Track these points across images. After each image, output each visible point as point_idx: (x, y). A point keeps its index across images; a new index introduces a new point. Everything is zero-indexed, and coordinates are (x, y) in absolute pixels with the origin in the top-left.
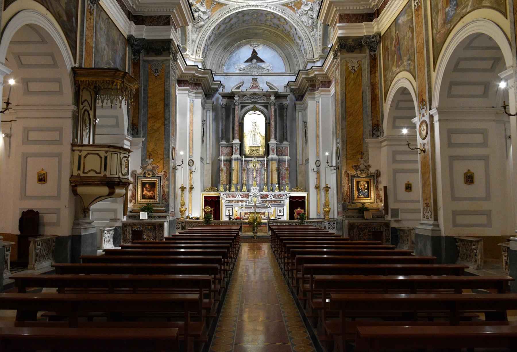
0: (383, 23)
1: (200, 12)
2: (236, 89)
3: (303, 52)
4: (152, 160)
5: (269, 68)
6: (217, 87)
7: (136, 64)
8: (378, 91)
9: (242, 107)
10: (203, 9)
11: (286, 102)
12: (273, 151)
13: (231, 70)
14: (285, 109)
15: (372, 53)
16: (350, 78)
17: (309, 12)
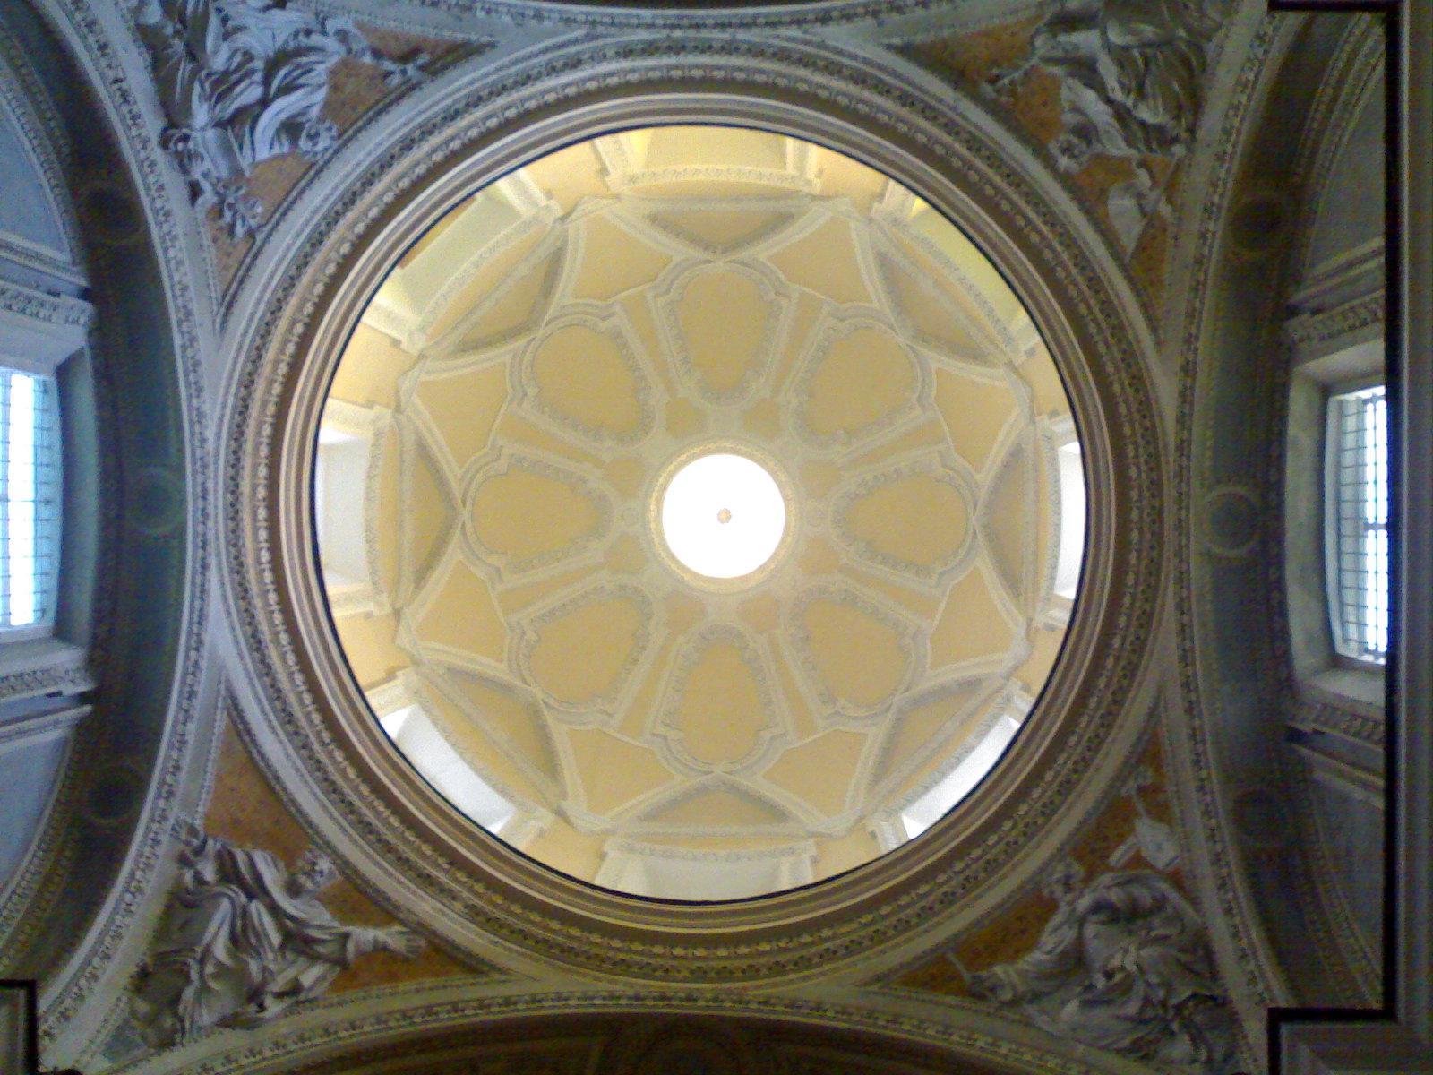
17: (249, 93)
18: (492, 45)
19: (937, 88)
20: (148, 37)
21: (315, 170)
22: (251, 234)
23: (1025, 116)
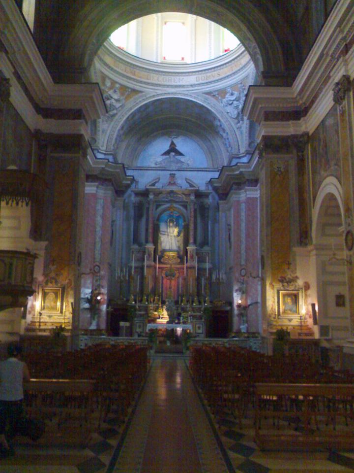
1: (113, 101)
2: (150, 186)
3: (228, 145)
4: (55, 267)
5: (189, 162)
6: (129, 182)
7: (41, 159)
8: (306, 195)
9: (158, 206)
10: (115, 96)
11: (209, 201)
13: (146, 164)
16: (277, 180)
17: (235, 102)
19: (138, 88)
20: (242, 120)
21: (231, 86)
22: (241, 83)
23: (123, 88)
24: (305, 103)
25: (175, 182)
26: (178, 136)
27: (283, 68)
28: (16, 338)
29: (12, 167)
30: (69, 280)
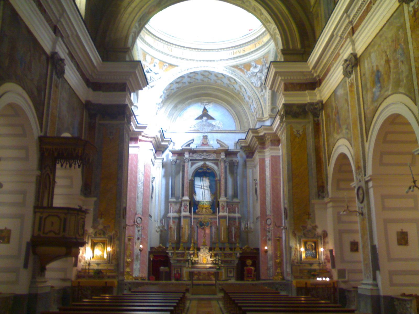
0: (325, 92)
4: (103, 219)
5: (219, 125)
6: (167, 143)
8: (322, 154)
12: (223, 208)
14: (236, 167)
15: (316, 119)
16: (296, 143)
17: (258, 74)
18: (230, 66)
22: (263, 58)
24: (318, 76)
25: (207, 143)
26: (209, 102)
27: (299, 46)
28: (68, 284)
29: (66, 135)
30: (116, 231)
